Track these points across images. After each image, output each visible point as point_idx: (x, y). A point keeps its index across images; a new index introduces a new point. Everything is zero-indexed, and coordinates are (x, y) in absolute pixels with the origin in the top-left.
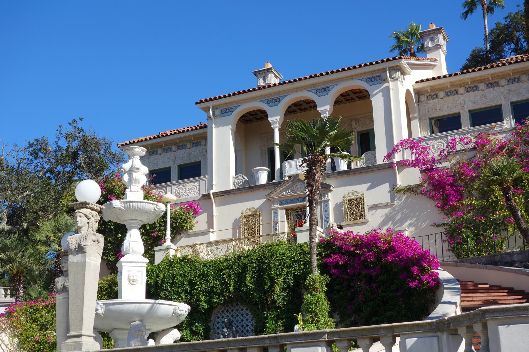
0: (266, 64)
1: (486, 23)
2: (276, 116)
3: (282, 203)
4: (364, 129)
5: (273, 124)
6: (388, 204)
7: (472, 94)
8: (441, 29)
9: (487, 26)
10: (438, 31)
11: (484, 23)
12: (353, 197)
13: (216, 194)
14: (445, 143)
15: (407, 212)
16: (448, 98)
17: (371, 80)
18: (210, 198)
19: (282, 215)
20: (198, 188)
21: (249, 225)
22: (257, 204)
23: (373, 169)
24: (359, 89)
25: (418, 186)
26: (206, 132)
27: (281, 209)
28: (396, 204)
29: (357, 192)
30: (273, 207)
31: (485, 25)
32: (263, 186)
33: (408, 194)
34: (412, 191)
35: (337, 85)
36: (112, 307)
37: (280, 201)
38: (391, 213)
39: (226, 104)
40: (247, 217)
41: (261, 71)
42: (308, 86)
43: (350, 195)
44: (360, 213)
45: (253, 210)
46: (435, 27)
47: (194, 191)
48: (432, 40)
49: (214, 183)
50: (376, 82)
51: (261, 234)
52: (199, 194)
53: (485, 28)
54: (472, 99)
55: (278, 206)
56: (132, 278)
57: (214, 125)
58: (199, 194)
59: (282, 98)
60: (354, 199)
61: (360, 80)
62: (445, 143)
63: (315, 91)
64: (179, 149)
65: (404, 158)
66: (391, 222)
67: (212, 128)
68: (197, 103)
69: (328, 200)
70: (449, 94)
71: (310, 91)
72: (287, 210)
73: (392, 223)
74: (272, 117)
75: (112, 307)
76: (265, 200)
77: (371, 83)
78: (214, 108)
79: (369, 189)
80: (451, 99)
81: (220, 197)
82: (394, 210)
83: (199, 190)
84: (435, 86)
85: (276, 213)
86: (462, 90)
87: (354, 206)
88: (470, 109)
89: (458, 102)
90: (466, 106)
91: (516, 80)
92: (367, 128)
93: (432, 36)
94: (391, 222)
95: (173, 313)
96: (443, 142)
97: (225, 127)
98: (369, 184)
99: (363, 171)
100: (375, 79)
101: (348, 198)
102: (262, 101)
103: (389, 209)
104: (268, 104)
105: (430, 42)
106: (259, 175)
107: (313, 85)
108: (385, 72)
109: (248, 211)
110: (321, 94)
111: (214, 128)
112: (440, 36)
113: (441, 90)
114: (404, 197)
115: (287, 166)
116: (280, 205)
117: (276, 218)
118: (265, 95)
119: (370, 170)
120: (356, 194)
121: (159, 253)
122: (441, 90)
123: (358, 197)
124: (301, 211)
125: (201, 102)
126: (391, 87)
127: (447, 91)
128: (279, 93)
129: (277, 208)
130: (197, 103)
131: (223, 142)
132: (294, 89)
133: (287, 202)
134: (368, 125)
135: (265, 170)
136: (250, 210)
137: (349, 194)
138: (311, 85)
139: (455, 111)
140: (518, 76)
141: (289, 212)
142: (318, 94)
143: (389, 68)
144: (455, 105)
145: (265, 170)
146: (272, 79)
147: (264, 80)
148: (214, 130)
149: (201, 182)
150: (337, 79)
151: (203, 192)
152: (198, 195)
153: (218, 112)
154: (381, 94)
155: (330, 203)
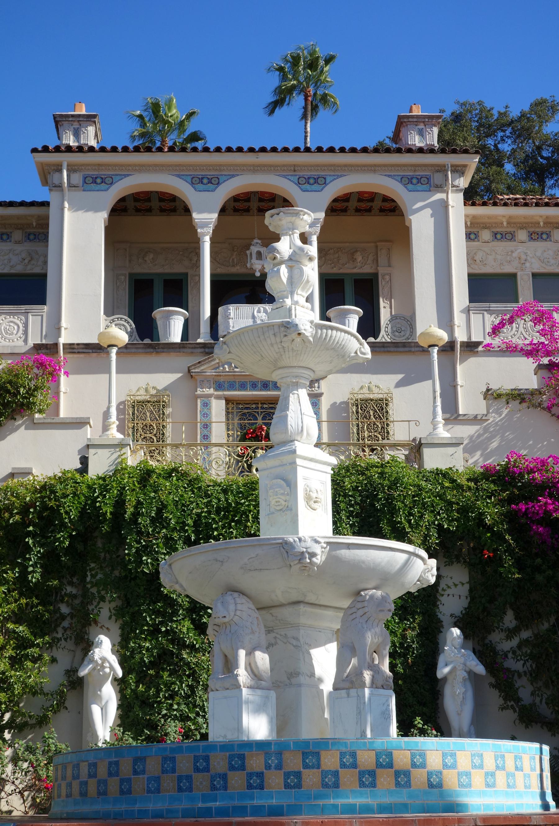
0: (78, 104)
1: (309, 129)
2: (210, 212)
3: (219, 386)
4: (335, 270)
5: (202, 227)
6: (476, 417)
7: (540, 245)
8: (95, 116)
9: (309, 134)
10: (90, 119)
11: (306, 128)
12: (371, 396)
13: (71, 348)
14: (21, 325)
15: (511, 437)
16: (495, 243)
17: (410, 181)
18: (57, 352)
19: (218, 408)
20: (21, 328)
21: (144, 418)
22: (162, 380)
23: (413, 349)
24: (272, 194)
25: (533, 393)
26: (47, 218)
27: (218, 398)
28: (491, 419)
29: (378, 387)
30: (199, 392)
31: (306, 132)
32: (172, 346)
33: (515, 404)
34: (523, 401)
35: (341, 176)
36: (344, 553)
37: (215, 382)
38: (479, 436)
39: (99, 166)
40: (142, 403)
41: (73, 116)
42: (284, 166)
43: (365, 390)
44: (383, 428)
45: (154, 392)
46: (84, 112)
47: (12, 334)
48: (421, 133)
49: (64, 323)
50: (419, 187)
51: (169, 441)
52: (26, 341)
53: (306, 137)
54: (539, 254)
55: (211, 391)
56: (314, 495)
57: (66, 205)
58: (26, 341)
59: (225, 178)
60: (372, 400)
61: (389, 176)
62: (21, 325)
63: (189, 179)
64: (531, 239)
65: (470, 337)
66: (478, 453)
67: (62, 209)
68: (35, 150)
69: (321, 395)
70: (499, 236)
71: (285, 176)
72: (228, 401)
73: (481, 455)
74: (200, 212)
75: (344, 553)
76: (180, 375)
77: (410, 186)
78: (72, 169)
79: (399, 384)
80: (502, 246)
81: (82, 356)
82: (486, 430)
83: (26, 332)
84: (481, 217)
85: (206, 405)
86: (522, 235)
87: (148, 414)
88: (536, 270)
89: (515, 255)
90: (528, 265)
91: (544, 236)
92: (341, 271)
93: (421, 126)
94: (478, 453)
95: (418, 580)
96: (18, 322)
97: (90, 214)
98: (400, 376)
99: (392, 349)
100: (419, 181)
101: (360, 396)
102: (179, 176)
103: (477, 427)
104: (192, 184)
105: (417, 138)
106: (172, 322)
107: (294, 168)
108: (60, 171)
109: (142, 392)
110: (307, 186)
111: (66, 210)
112: (91, 130)
113: (485, 227)
114: (505, 412)
115: (232, 316)
116: (216, 390)
117: (206, 415)
118: (210, 166)
119: (407, 349)
120: (375, 390)
121: (100, 451)
122: (485, 227)
123: (381, 396)
124: (257, 408)
125: (45, 149)
126: (451, 202)
127: (495, 230)
128: (219, 167)
129: (210, 396)
130: (35, 150)
131: (81, 242)
132: (254, 166)
133: (232, 387)
134: (343, 265)
135: (182, 314)
136: (146, 390)
137: (138, 390)
138: (290, 166)
139: (508, 269)
140: (512, 230)
141: (231, 405)
142: (196, 186)
143: (452, 166)
144: (508, 258)
145: (182, 314)
146: (90, 137)
147: (77, 135)
148: (67, 214)
149: (30, 317)
150: (345, 166)
151: (34, 339)
152: (21, 343)
153: (77, 178)
154: (429, 211)
155: (323, 399)
